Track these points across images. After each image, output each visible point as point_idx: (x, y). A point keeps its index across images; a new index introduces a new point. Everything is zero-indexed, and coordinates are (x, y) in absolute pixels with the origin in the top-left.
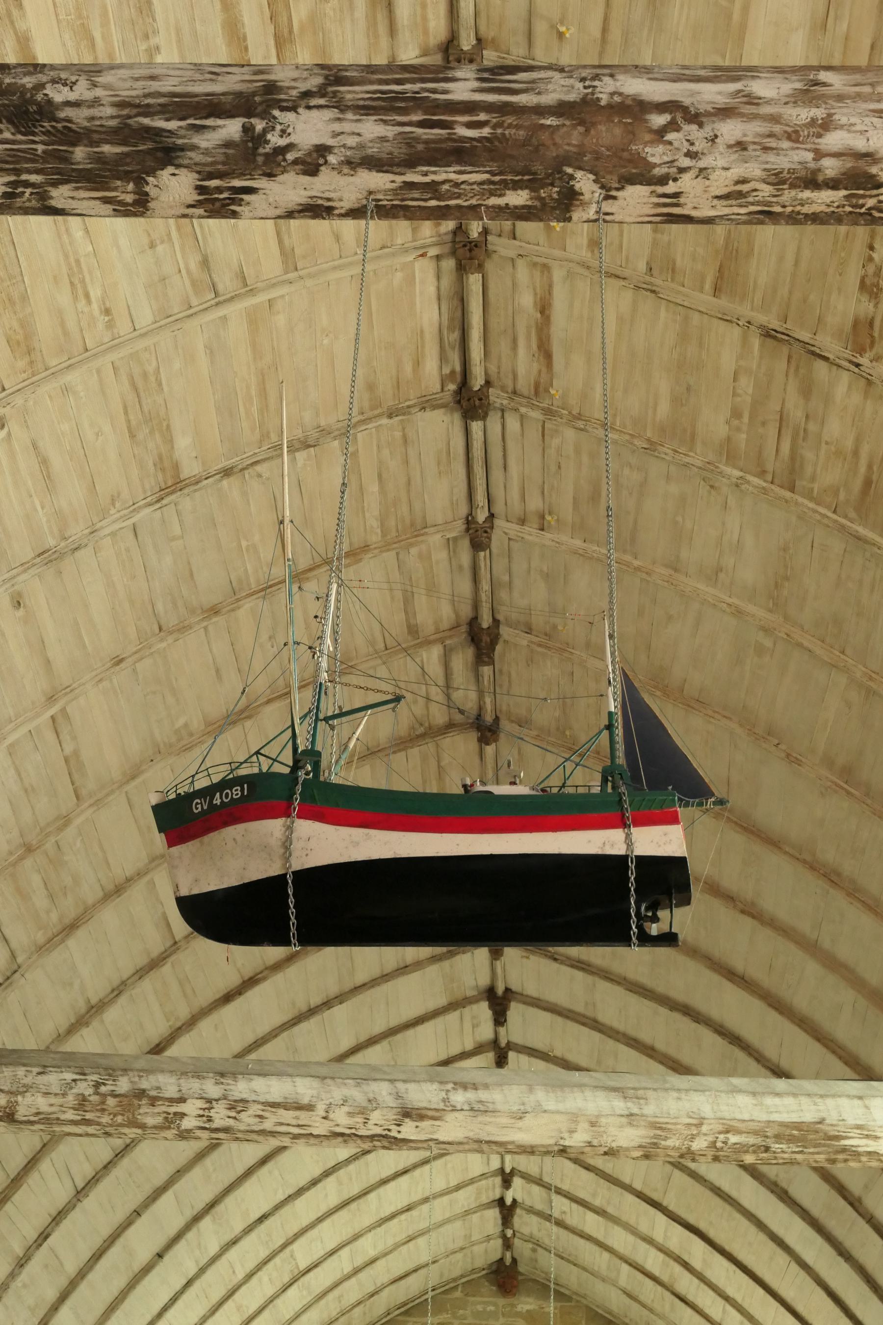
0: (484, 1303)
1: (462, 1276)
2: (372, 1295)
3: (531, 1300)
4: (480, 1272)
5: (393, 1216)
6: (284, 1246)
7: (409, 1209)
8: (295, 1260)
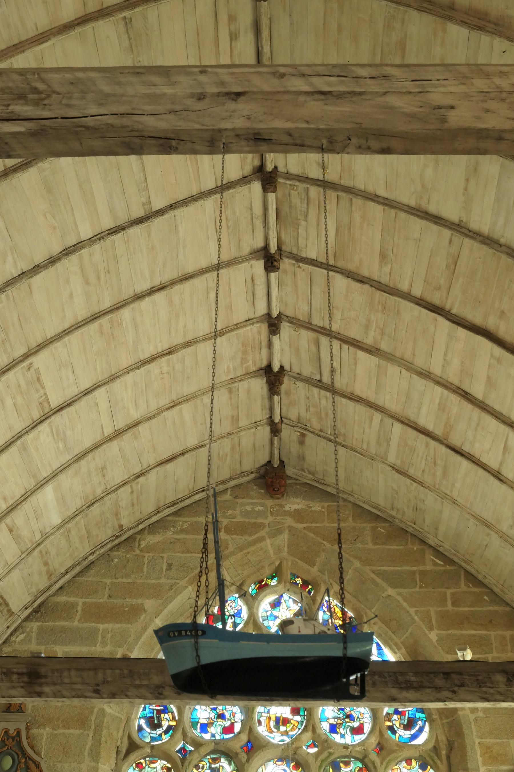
0: (252, 504)
1: (231, 479)
2: (138, 476)
3: (298, 500)
4: (248, 475)
5: (153, 359)
6: (26, 356)
7: (170, 352)
8: (43, 388)
